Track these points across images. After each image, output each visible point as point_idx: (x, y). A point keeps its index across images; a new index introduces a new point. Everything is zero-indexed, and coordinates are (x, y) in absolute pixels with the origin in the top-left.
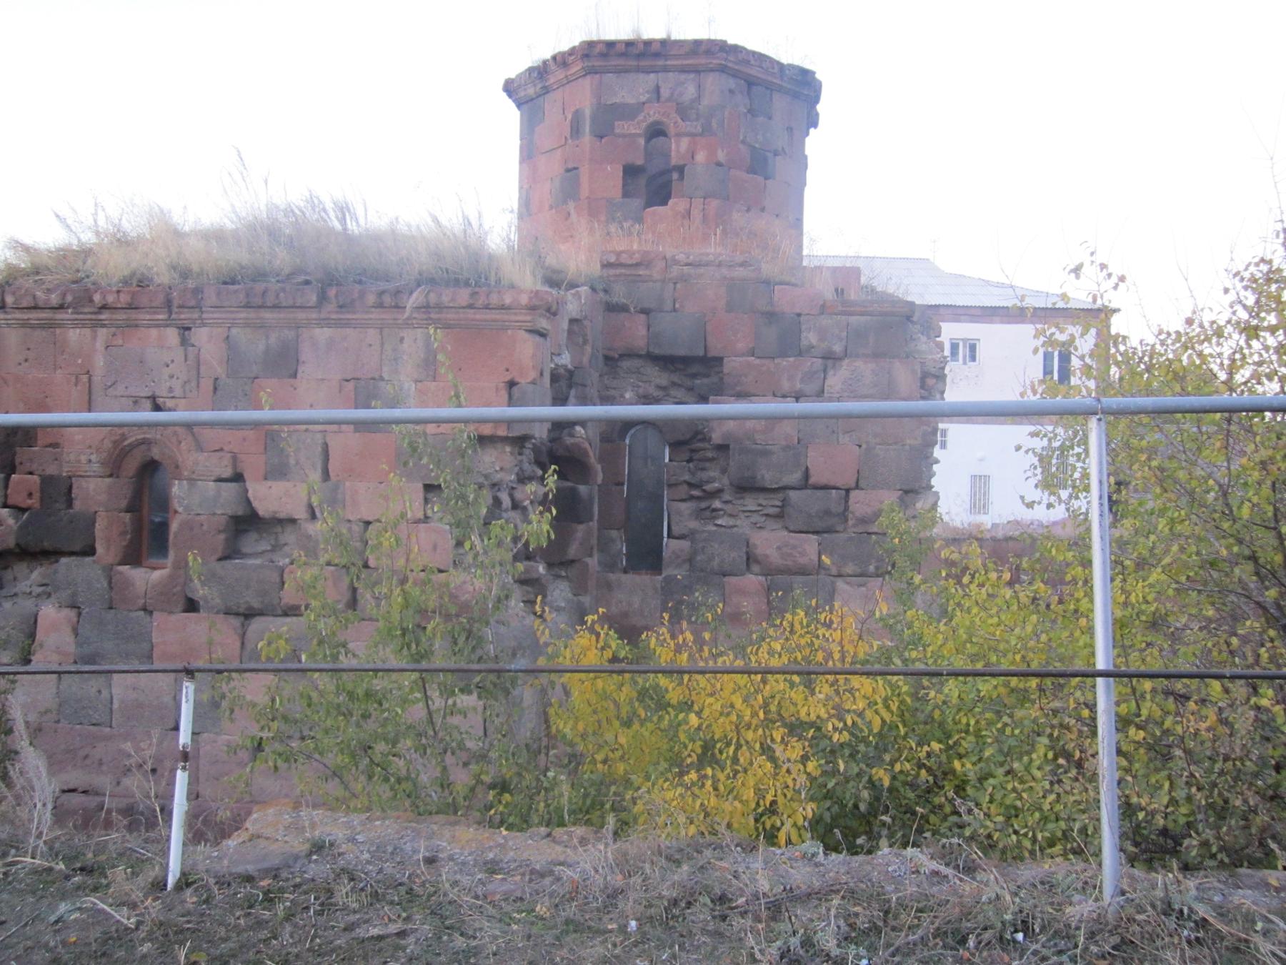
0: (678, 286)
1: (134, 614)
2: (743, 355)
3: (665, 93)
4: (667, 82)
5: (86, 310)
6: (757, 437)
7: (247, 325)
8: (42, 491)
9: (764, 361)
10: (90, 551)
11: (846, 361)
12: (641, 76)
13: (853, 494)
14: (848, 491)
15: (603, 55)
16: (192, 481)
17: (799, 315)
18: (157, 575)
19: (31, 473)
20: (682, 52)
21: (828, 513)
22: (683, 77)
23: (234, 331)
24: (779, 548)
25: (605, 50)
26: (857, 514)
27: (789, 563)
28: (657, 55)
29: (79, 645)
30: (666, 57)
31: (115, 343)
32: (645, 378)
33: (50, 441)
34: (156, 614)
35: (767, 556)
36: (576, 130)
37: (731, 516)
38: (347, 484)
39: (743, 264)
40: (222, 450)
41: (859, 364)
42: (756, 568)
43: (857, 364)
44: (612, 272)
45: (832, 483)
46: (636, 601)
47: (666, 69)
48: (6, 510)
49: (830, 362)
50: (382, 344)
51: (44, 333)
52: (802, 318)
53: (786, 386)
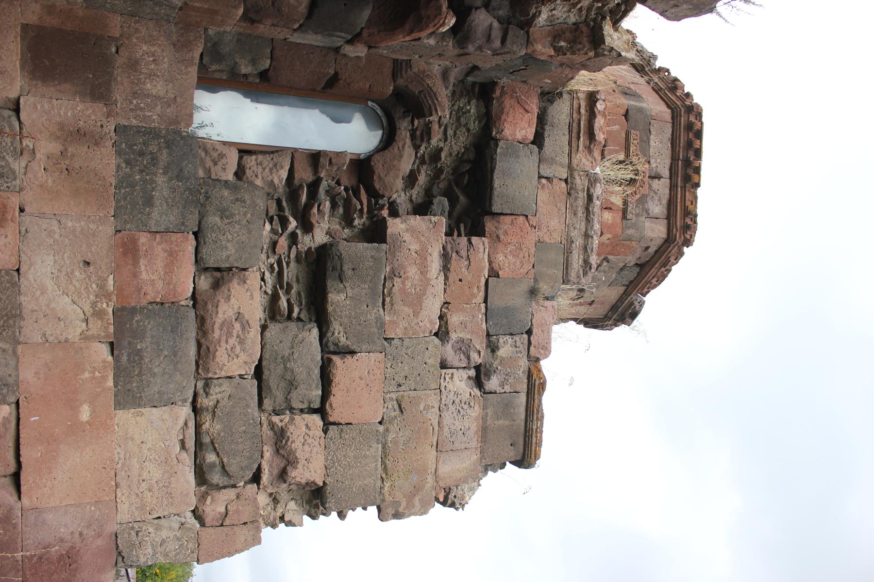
0: (563, 184)
2: (490, 262)
3: (656, 184)
4: (662, 187)
6: (397, 281)
9: (483, 289)
11: (476, 392)
12: (668, 162)
13: (316, 419)
14: (321, 411)
15: (690, 127)
17: (529, 332)
20: (688, 203)
21: (292, 385)
22: (665, 202)
24: (239, 316)
25: (696, 128)
26: (291, 428)
27: (217, 334)
30: (684, 188)
32: (450, 132)
35: (228, 298)
36: (627, 93)
37: (274, 245)
39: (586, 263)
41: (476, 411)
42: (204, 283)
43: (477, 408)
44: (583, 104)
45: (334, 390)
46: (156, 87)
47: (673, 187)
49: (472, 373)
52: (525, 336)
53: (454, 319)
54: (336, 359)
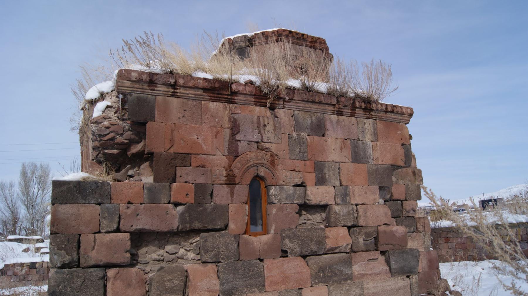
1: (254, 261)
5: (224, 93)
7: (303, 110)
8: (196, 192)
10: (226, 227)
16: (282, 186)
18: (265, 238)
19: (186, 182)
23: (296, 112)
28: (304, 39)
29: (222, 284)
31: (236, 112)
33: (199, 164)
34: (265, 260)
38: (351, 187)
40: (294, 170)
48: (170, 205)
50: (358, 124)
51: (195, 103)
54: (394, 198)
